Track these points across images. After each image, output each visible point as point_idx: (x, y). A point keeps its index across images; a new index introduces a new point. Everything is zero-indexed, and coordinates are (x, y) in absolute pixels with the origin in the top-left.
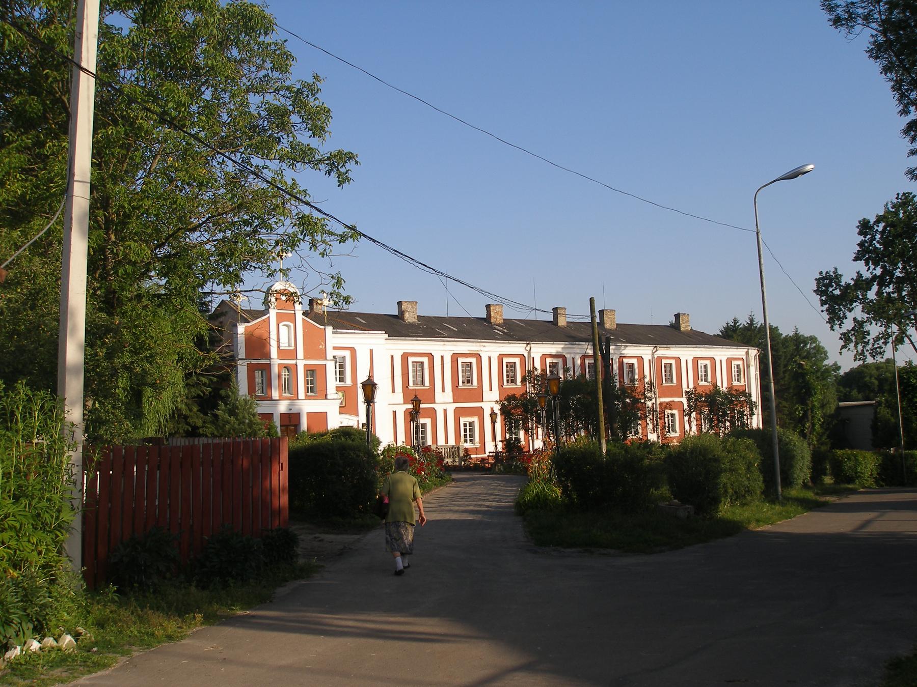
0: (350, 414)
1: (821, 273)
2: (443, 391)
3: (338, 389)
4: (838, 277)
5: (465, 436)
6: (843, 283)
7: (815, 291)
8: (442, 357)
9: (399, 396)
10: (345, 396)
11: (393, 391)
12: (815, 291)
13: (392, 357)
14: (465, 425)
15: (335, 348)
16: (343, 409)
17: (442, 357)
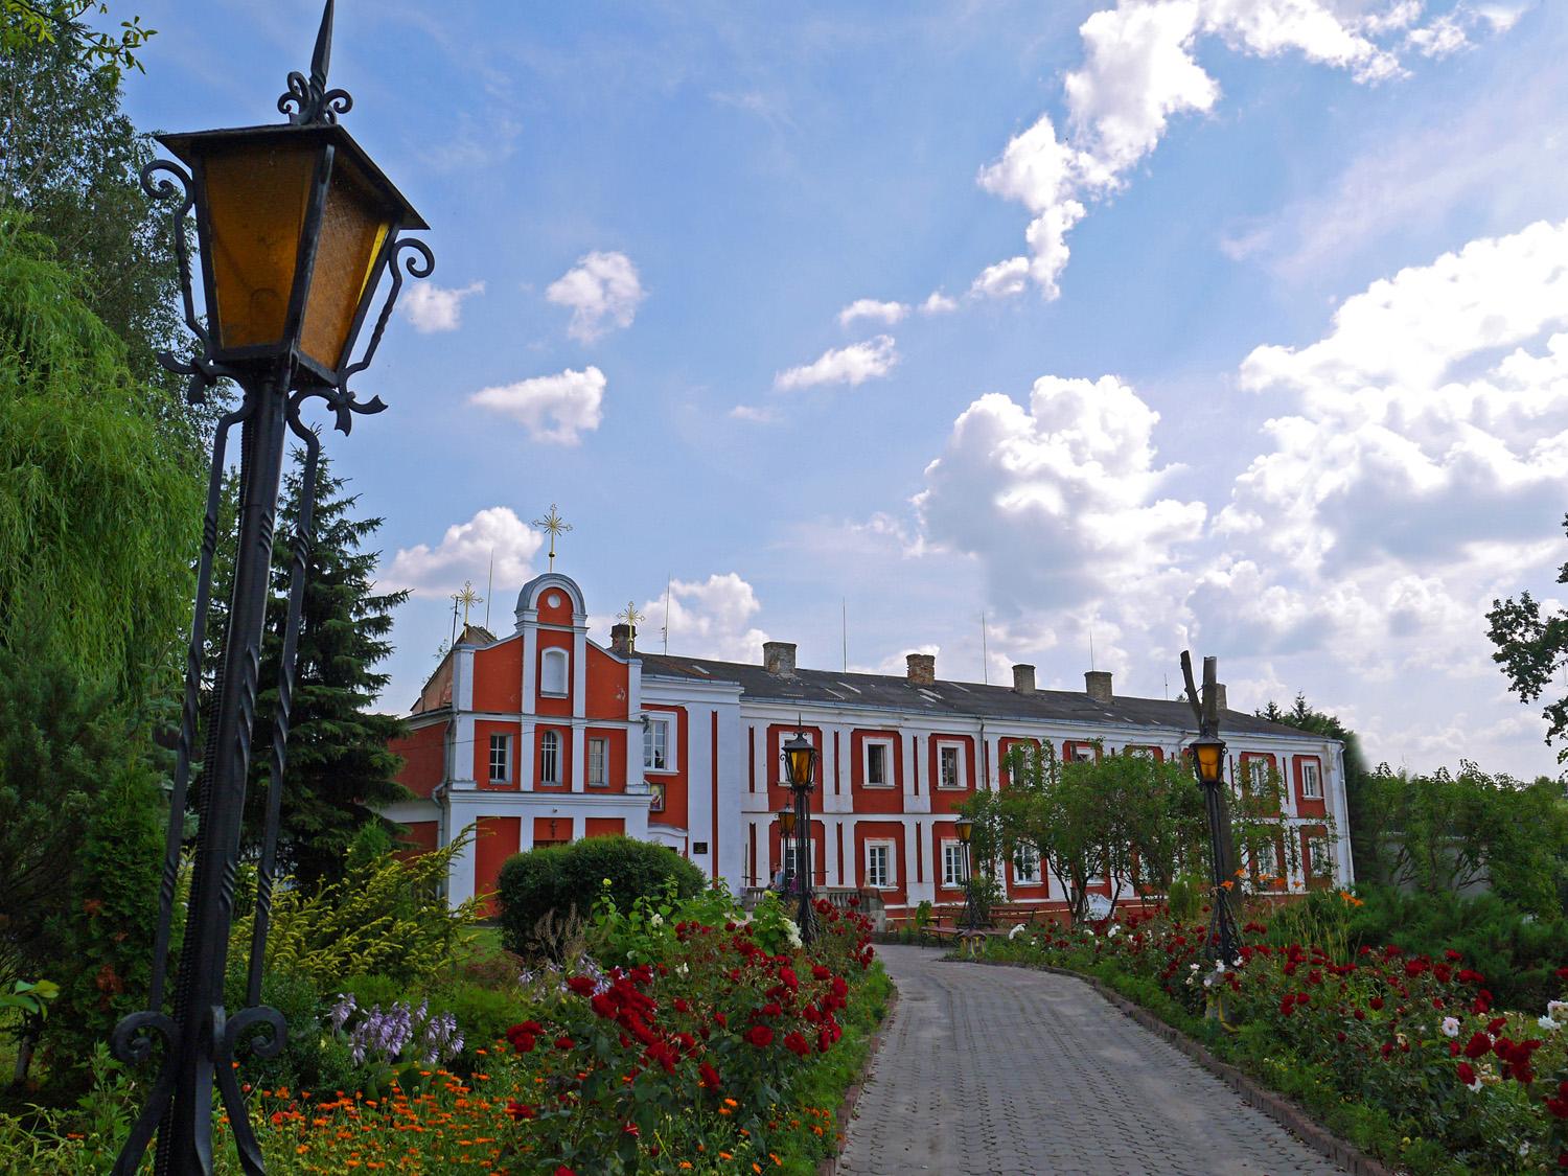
0: (674, 826)
1: (1496, 603)
2: (837, 792)
3: (651, 779)
4: (1532, 608)
5: (873, 871)
6: (1542, 620)
7: (1489, 635)
8: (836, 734)
9: (762, 799)
10: (664, 793)
11: (752, 790)
12: (1489, 635)
13: (751, 730)
14: (873, 852)
15: (644, 706)
16: (655, 817)
17: (836, 734)
